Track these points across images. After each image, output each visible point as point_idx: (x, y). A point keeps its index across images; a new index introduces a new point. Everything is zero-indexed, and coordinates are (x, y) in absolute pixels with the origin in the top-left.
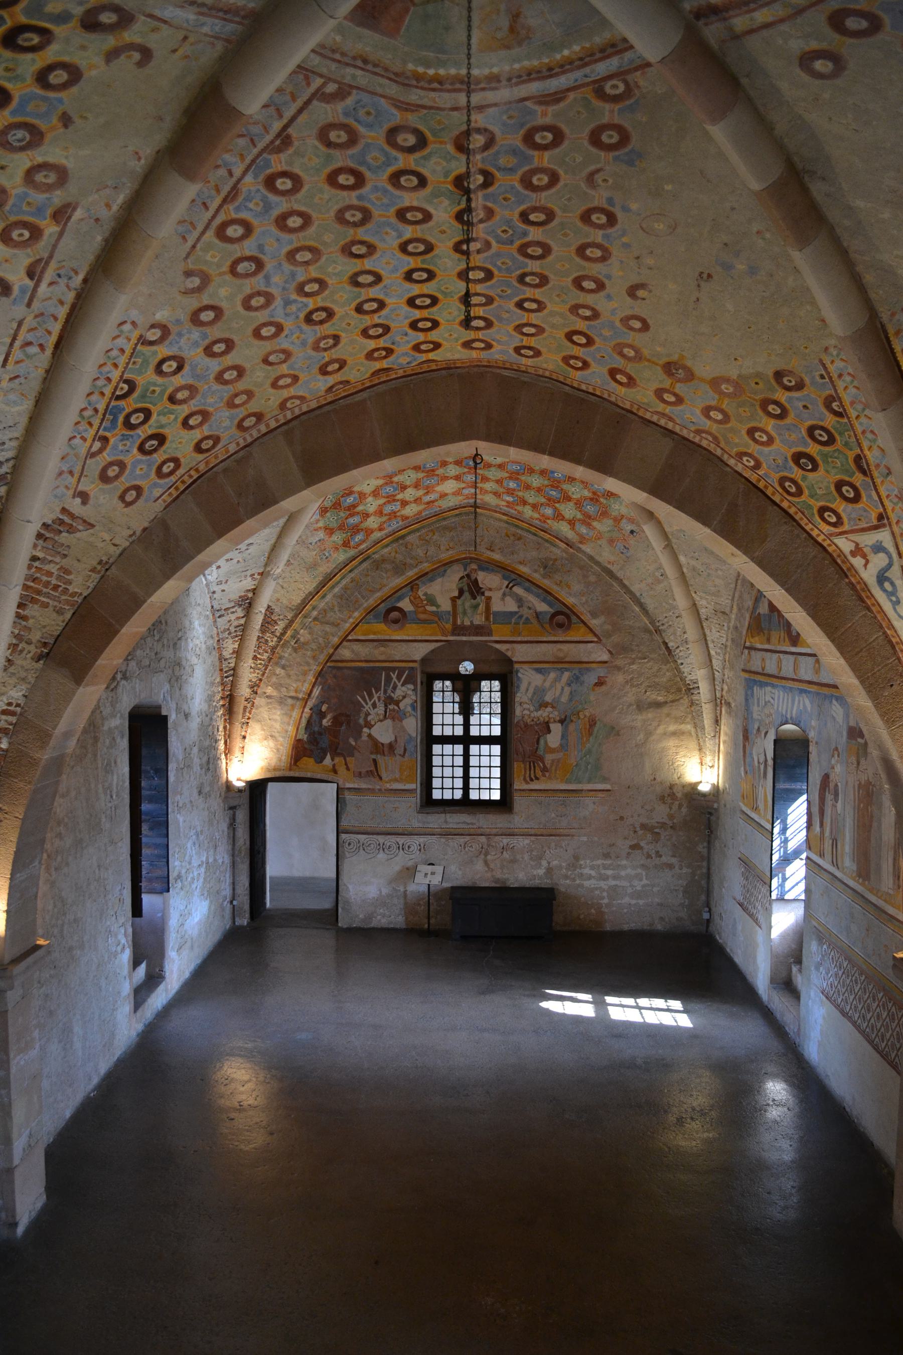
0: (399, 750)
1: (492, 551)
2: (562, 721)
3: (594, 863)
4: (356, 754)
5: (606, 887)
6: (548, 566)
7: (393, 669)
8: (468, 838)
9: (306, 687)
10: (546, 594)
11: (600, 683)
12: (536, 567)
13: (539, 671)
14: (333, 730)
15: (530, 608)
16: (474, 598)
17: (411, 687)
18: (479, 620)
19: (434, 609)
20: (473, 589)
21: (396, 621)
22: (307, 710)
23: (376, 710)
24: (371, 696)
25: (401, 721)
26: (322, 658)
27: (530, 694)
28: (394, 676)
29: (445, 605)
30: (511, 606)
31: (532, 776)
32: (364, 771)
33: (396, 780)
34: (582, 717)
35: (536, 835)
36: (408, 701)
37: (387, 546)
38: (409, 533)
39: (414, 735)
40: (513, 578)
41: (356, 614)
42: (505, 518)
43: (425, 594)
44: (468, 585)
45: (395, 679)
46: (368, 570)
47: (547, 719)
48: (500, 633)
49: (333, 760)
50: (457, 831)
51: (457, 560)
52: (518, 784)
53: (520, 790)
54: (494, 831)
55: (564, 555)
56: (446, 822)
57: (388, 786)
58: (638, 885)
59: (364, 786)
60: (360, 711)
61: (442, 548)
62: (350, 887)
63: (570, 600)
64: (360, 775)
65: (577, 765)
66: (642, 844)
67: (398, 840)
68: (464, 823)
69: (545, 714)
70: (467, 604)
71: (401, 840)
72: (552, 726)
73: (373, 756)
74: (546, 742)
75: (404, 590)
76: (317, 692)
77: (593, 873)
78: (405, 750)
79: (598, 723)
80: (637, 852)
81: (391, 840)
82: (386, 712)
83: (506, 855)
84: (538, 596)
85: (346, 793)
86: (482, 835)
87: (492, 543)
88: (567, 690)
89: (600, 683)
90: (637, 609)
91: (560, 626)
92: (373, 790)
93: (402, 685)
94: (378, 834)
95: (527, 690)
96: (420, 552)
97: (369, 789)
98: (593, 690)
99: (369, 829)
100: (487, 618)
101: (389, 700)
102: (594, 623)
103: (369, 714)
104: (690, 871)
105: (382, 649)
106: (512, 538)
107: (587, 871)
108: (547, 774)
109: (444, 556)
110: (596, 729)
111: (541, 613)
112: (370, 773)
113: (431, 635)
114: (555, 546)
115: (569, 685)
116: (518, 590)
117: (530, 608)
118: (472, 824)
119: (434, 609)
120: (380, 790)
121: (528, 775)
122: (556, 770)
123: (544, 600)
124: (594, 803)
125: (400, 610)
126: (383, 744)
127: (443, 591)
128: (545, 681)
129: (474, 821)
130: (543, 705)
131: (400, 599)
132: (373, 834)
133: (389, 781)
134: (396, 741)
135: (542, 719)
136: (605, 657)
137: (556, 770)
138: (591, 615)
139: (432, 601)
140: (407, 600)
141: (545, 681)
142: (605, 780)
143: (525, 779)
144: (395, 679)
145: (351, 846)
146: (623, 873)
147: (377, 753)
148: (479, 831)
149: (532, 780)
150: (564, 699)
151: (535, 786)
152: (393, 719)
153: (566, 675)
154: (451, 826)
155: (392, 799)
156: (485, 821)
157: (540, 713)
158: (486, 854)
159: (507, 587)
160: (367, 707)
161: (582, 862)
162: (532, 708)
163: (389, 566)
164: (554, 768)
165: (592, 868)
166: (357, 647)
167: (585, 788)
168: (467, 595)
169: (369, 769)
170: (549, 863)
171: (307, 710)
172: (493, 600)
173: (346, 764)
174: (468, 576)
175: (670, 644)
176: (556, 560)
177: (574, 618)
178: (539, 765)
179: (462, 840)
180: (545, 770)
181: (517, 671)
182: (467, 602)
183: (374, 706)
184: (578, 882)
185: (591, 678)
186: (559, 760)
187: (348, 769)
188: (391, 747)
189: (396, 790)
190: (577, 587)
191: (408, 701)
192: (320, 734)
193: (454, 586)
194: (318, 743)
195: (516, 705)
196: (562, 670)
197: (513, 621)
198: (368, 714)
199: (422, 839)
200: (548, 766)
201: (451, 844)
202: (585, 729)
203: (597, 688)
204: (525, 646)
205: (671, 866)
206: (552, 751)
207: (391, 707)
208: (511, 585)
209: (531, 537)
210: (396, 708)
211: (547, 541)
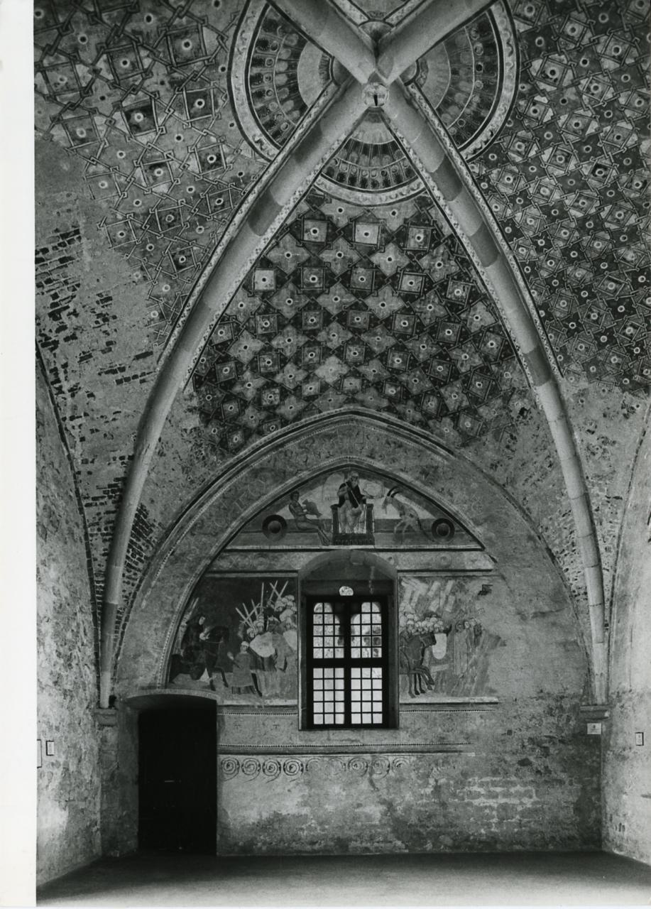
0: (280, 665)
1: (373, 458)
2: (447, 632)
3: (483, 780)
4: (235, 668)
5: (496, 806)
6: (429, 473)
7: (273, 580)
8: (351, 757)
9: (183, 599)
10: (429, 503)
11: (485, 591)
12: (417, 475)
13: (422, 579)
14: (211, 646)
15: (412, 516)
16: (356, 506)
17: (292, 598)
18: (361, 530)
19: (314, 517)
20: (354, 496)
21: (275, 530)
22: (184, 623)
23: (255, 622)
24: (250, 609)
25: (281, 632)
26: (200, 568)
27: (413, 605)
28: (274, 588)
29: (326, 513)
30: (392, 514)
31: (418, 690)
32: (243, 687)
33: (276, 696)
34: (467, 627)
35: (422, 752)
36: (288, 613)
37: (265, 454)
38: (288, 441)
39: (295, 648)
40: (396, 485)
41: (234, 524)
42: (385, 425)
43: (306, 502)
44: (349, 493)
46: (246, 478)
47: (431, 629)
48: (382, 540)
49: (210, 676)
50: (339, 750)
51: (338, 468)
52: (404, 698)
53: (406, 704)
54: (378, 749)
55: (446, 463)
56: (329, 739)
57: (268, 702)
58: (528, 803)
59: (243, 703)
61: (322, 455)
62: (229, 812)
63: (454, 508)
64: (239, 691)
65: (463, 677)
66: (532, 759)
67: (279, 760)
68: (349, 740)
69: (430, 624)
70: (349, 513)
71: (283, 760)
72: (437, 637)
73: (252, 671)
74: (431, 653)
75: (283, 498)
76: (194, 605)
77: (482, 791)
79: (484, 632)
80: (525, 769)
81: (271, 761)
82: (265, 624)
83: (392, 774)
84: (419, 503)
85: (225, 710)
86: (366, 753)
87: (373, 450)
88: (452, 599)
89: (485, 591)
90: (518, 515)
91: (443, 533)
93: (283, 596)
94: (258, 754)
95: (411, 599)
96: (300, 460)
97: (248, 706)
98: (478, 599)
99: (249, 749)
100: (369, 528)
101: (269, 612)
102: (478, 531)
103: (248, 627)
104: (580, 786)
105: (261, 559)
106: (393, 445)
107: (476, 788)
108: (433, 687)
109: (326, 463)
110: (482, 639)
111: (423, 520)
112: (249, 690)
113: (311, 544)
114: (437, 453)
115: (453, 593)
116: (398, 497)
117: (412, 516)
118: (356, 741)
119: (314, 517)
120: (260, 707)
121: (413, 688)
122: (441, 683)
123: (426, 508)
124: (481, 717)
125: (280, 519)
126: (262, 658)
127: (323, 499)
128: (429, 590)
129: (359, 738)
130: (428, 615)
131: (279, 507)
132: (253, 754)
133: (269, 698)
134: (276, 654)
135: (426, 629)
136: (490, 566)
137: (441, 683)
138: (474, 523)
139: (312, 509)
140: (287, 508)
141: (429, 590)
142: (492, 692)
143: (410, 692)
145: (230, 768)
146: (512, 790)
148: (363, 749)
149: (417, 693)
150: (448, 609)
151: (421, 699)
152: (273, 631)
153: (450, 584)
154: (334, 743)
156: (370, 739)
157: (424, 623)
158: (371, 774)
159: (388, 495)
160: (246, 620)
161: (470, 780)
162: (416, 618)
163: (268, 474)
164: (439, 681)
165: (481, 785)
166: (236, 559)
167: (471, 701)
168: (348, 502)
169: (248, 685)
170: (436, 781)
171: (184, 623)
172: (375, 508)
173: (224, 680)
174: (349, 483)
175: (554, 550)
176: (437, 467)
177: (457, 527)
178: (424, 677)
179: (346, 758)
180: (430, 682)
181: (400, 581)
182: (348, 511)
183: (254, 618)
184: (466, 801)
185: (475, 587)
186: (444, 673)
187: (226, 685)
188: (271, 661)
189: (276, 706)
190: (458, 495)
192: (197, 648)
193: (335, 494)
195: (400, 614)
196: (446, 579)
197: (395, 529)
198: (247, 627)
199: (304, 759)
200: (434, 678)
201: (335, 763)
202: (471, 638)
203: (481, 597)
204: (409, 555)
205: (561, 782)
206: (437, 662)
207: (271, 619)
208: (392, 493)
209: (412, 444)
210: (276, 619)
211: (428, 448)
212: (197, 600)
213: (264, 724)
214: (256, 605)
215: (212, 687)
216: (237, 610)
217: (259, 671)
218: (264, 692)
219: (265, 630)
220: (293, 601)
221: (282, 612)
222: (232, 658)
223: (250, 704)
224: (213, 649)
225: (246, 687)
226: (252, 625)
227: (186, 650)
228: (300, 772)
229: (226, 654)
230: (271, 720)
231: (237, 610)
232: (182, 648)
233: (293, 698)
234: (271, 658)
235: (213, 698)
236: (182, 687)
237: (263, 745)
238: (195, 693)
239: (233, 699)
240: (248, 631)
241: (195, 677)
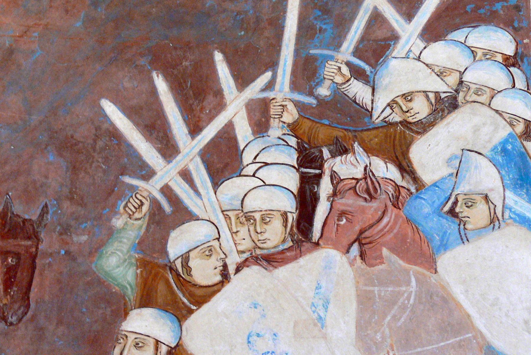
23: (233, 188)
24: (199, 97)
25: (422, 253)
60: (112, 194)
82: (306, 201)
93: (433, 32)
101: (324, 132)
103: (183, 215)
152: (364, 245)
160: (166, 173)
183: (223, 160)
198: (170, 215)
207: (348, 167)
210: (385, 170)
214: (243, 81)
216: (111, 110)
220: (509, 62)
221: (424, 127)
226: (206, 200)
231: (111, 110)
240: (179, 242)
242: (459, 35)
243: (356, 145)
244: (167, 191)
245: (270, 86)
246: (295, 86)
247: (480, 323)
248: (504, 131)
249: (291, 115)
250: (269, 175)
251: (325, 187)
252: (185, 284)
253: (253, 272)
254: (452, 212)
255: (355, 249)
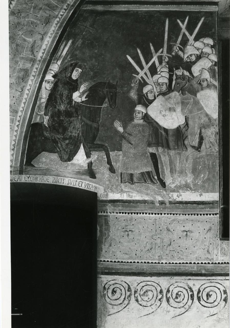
4: (125, 145)
7: (182, 15)
9: (47, 42)
17: (210, 41)
23: (156, 77)
25: (194, 92)
28: (183, 26)
32: (137, 172)
33: (187, 187)
36: (205, 64)
45: (184, 30)
49: (88, 155)
57: (175, 196)
59: (137, 197)
64: (131, 179)
67: (191, 283)
71: (196, 284)
73: (152, 150)
76: (65, 50)
78: (201, 139)
81: (178, 285)
82: (170, 80)
85: (109, 208)
92: (153, 203)
93: (196, 39)
94: (159, 274)
97: (145, 202)
99: (145, 267)
101: (176, 63)
112: (146, 177)
120: (162, 203)
126: (166, 130)
133: (177, 189)
144: (184, 30)
145: (117, 295)
147: (157, 144)
152: (182, 90)
155: (182, 217)
160: (142, 73)
169: (145, 170)
171: (49, 77)
173: (109, 162)
187: (112, 170)
188: (179, 135)
189: (187, 203)
191: (205, 64)
192: (68, 114)
194: (65, 129)
198: (143, 84)
207: (179, 72)
210: (186, 73)
212: (70, 42)
213: (168, 230)
214: (156, 51)
215: (91, 172)
217: (160, 149)
218: (168, 181)
219: (170, 89)
221: (194, 63)
222: (121, 129)
223: (147, 198)
224: (94, 115)
225: (142, 174)
226: (150, 80)
227: (52, 117)
228: (223, 303)
229: (113, 124)
230: (180, 222)
232: (45, 114)
233: (213, 191)
234: (178, 130)
235: (92, 190)
236: (46, 172)
237: (167, 261)
238: (69, 180)
239: (122, 191)
240: (145, 90)
241: (66, 157)
242: (201, 40)
243: (180, 67)
244: (142, 77)
245: (162, 52)
246: (167, 53)
247: (205, 109)
248: (211, 64)
249: (167, 60)
250: (163, 74)
251: (174, 77)
252: (147, 99)
253: (161, 97)
254: (200, 83)
255: (180, 92)
